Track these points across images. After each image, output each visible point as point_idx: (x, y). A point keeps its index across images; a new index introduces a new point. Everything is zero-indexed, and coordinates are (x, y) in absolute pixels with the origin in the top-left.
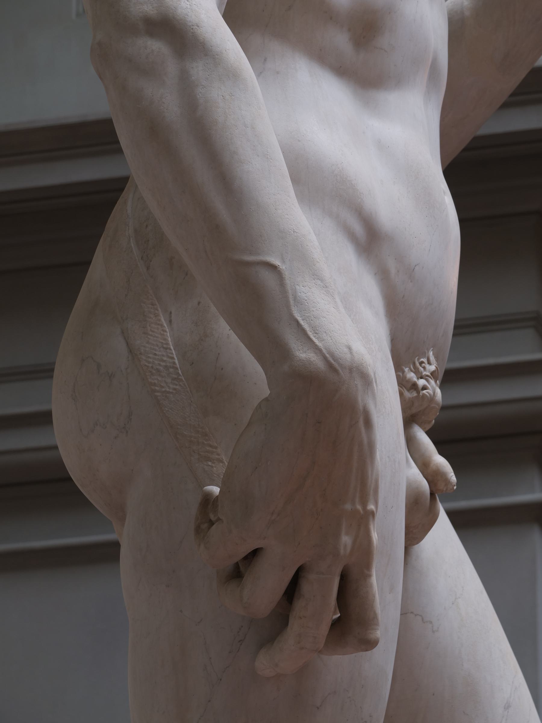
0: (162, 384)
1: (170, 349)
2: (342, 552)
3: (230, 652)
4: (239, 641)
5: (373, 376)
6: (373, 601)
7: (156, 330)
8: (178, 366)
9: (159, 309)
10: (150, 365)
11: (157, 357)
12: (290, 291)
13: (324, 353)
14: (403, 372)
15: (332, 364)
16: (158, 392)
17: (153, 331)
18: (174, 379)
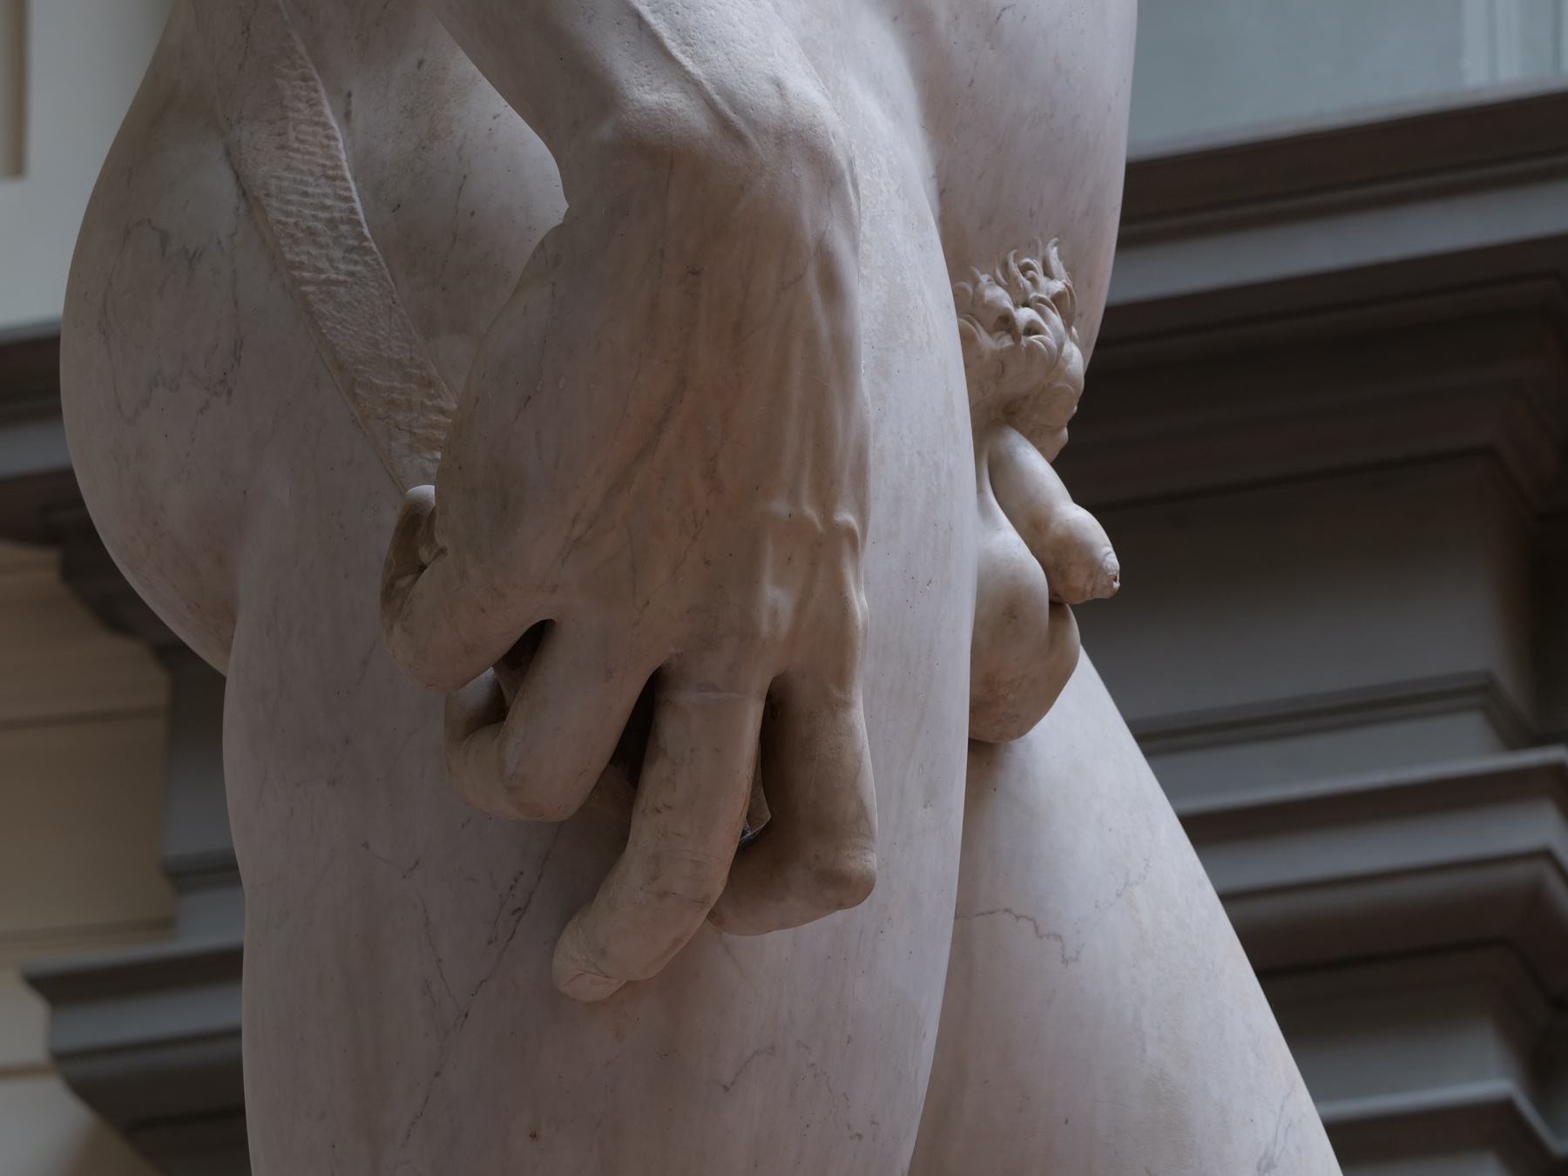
0: (320, 265)
1: (344, 179)
2: (765, 628)
3: (490, 942)
4: (515, 912)
5: (844, 164)
6: (857, 771)
8: (362, 217)
10: (291, 220)
11: (309, 200)
13: (707, 93)
14: (976, 282)
15: (730, 121)
16: (309, 282)
17: (302, 142)
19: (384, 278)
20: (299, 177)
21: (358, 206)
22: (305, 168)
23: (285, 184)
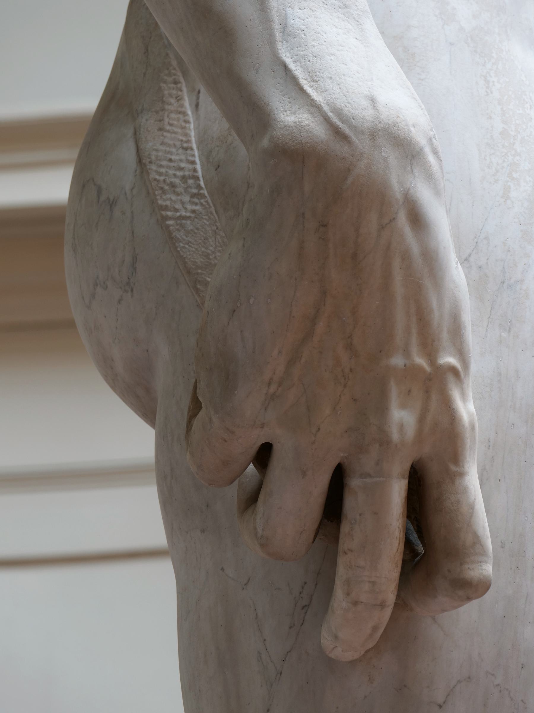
0: (177, 207)
1: (192, 149)
2: (395, 436)
4: (303, 608)
7: (175, 122)
8: (200, 174)
9: (185, 89)
10: (162, 178)
11: (172, 164)
12: (276, 19)
13: (324, 112)
16: (170, 218)
17: (171, 125)
18: (193, 196)
19: (211, 213)
20: (168, 149)
21: (198, 167)
22: (172, 143)
23: (160, 154)
